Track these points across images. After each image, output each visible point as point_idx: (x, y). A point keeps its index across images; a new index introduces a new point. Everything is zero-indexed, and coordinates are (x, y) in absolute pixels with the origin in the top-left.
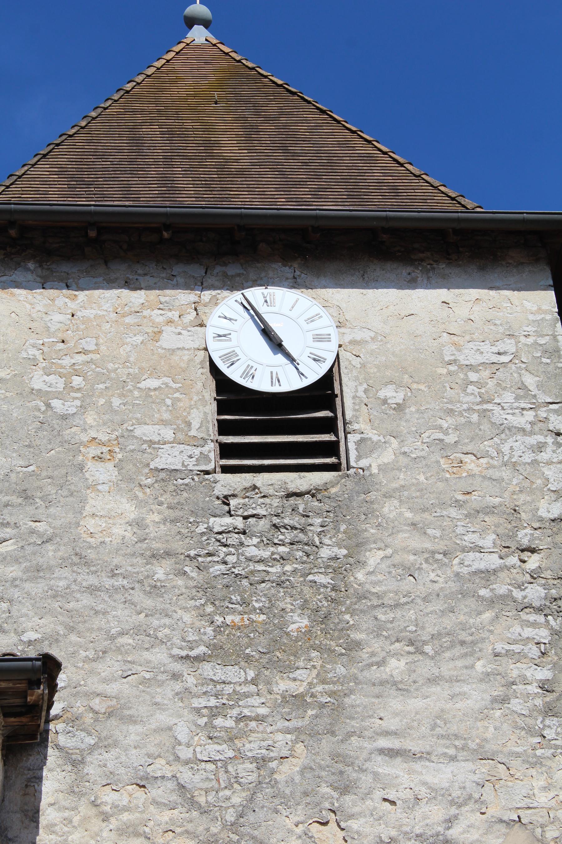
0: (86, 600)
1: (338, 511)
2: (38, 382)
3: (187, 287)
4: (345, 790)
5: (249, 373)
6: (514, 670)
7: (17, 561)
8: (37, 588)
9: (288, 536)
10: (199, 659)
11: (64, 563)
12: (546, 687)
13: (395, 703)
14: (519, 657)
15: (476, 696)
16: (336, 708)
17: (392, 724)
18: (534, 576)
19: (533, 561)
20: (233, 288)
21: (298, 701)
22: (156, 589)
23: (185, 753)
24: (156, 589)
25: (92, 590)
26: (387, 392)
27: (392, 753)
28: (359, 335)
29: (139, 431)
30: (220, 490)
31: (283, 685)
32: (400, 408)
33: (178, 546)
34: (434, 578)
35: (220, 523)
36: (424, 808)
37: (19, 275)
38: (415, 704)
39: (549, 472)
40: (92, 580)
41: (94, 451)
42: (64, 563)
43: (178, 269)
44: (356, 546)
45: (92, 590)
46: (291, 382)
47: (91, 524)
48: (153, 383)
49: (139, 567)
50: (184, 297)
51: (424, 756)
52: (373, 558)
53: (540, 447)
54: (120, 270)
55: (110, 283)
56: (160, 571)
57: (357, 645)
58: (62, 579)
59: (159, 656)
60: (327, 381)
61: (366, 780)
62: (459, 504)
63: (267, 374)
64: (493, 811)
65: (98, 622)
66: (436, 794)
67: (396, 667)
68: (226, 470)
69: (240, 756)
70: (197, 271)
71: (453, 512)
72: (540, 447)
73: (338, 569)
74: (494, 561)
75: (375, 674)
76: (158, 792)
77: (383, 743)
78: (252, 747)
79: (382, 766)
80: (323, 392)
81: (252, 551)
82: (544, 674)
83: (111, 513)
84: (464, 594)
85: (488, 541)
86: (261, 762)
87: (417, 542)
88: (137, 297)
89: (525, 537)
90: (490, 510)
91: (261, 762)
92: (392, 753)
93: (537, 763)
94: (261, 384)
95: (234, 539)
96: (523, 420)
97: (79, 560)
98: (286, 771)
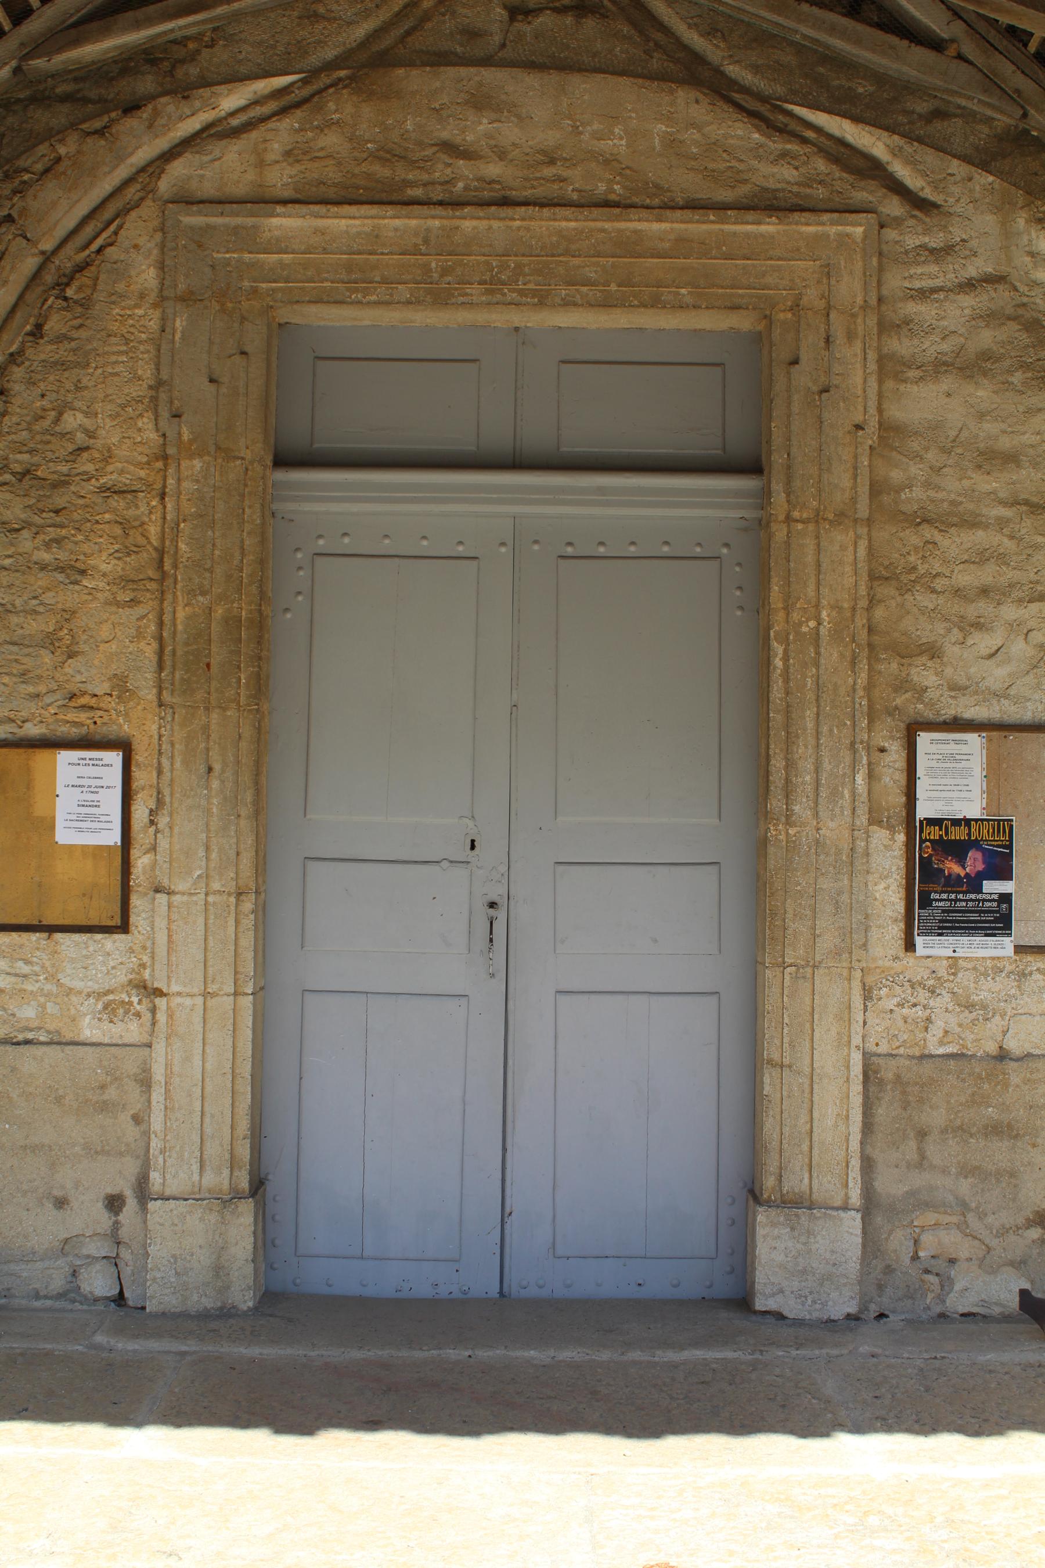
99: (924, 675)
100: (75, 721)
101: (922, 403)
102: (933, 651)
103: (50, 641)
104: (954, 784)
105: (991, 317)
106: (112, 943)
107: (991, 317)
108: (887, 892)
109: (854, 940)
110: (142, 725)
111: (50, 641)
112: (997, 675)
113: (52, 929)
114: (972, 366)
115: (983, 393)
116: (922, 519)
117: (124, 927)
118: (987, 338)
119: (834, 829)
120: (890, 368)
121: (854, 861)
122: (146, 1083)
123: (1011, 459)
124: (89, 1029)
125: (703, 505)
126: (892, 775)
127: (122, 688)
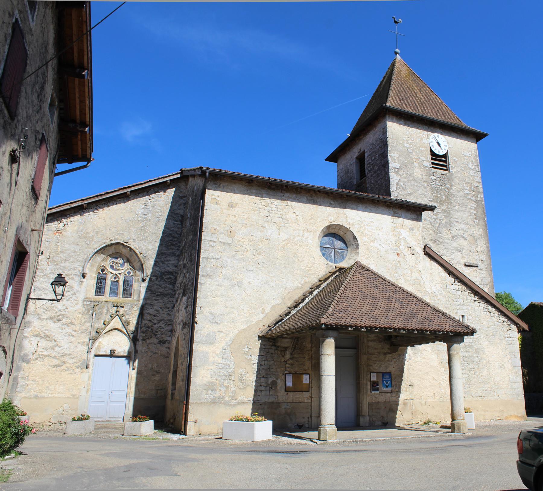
0: (415, 188)
1: (449, 179)
2: (406, 145)
3: (426, 130)
4: (451, 226)
5: (435, 150)
6: (471, 211)
7: (406, 178)
8: (409, 184)
9: (442, 182)
10: (431, 201)
11: (412, 180)
12: (475, 214)
13: (457, 214)
14: (472, 209)
15: (467, 214)
16: (449, 213)
17: (456, 217)
18: (474, 195)
19: (474, 193)
20: (432, 132)
21: (445, 211)
22: (425, 188)
23: (430, 217)
24: (425, 188)
25: (417, 186)
26: (454, 158)
27: (457, 222)
28: (451, 146)
29: (421, 158)
30: (432, 171)
31: (442, 208)
32: (456, 161)
33: (427, 180)
34: (461, 193)
35: (433, 177)
36: (461, 231)
37: (401, 122)
38: (459, 214)
39: (476, 178)
40: (416, 184)
41: (414, 160)
42: (412, 180)
43: (424, 126)
44: (451, 186)
45: (417, 186)
46: (441, 153)
47: (415, 174)
48: (422, 149)
49: (422, 183)
50: (426, 132)
51: (460, 223)
52: (454, 188)
53: (475, 173)
54: (416, 125)
55: (415, 127)
56: (425, 184)
57: (451, 203)
58: (412, 183)
59: (426, 199)
60: (446, 154)
61: (453, 225)
62: (464, 181)
63: (439, 151)
64: (469, 233)
65: (418, 192)
66: (462, 229)
67: (457, 207)
68: (433, 167)
69: (437, 218)
70: (427, 127)
71: (463, 182)
72: (475, 173)
73: (450, 189)
74: (468, 192)
75: (454, 208)
76: (428, 222)
77: (455, 220)
78: (439, 217)
79: (455, 223)
80: (445, 156)
81: (437, 183)
82: (475, 212)
83: (418, 173)
84: (466, 197)
85: (468, 188)
86: (440, 220)
87: (459, 187)
88: (419, 131)
89: (473, 188)
90: (468, 183)
91: (440, 220)
92: (457, 222)
93: (474, 226)
94: (437, 152)
95: (435, 181)
96: (473, 168)
97: (414, 180)
98: (443, 222)
99: (371, 368)
100: (305, 372)
101: (371, 344)
102: (372, 366)
103: (302, 364)
104: (374, 378)
105: (375, 336)
106: (308, 393)
107: (375, 336)
108: (369, 387)
109: (367, 392)
110: (310, 373)
111: (302, 364)
112: (377, 368)
113: (302, 391)
114: (374, 341)
115: (375, 343)
116: (370, 354)
117: (309, 391)
118: (375, 338)
119: (365, 382)
120: (368, 341)
121: (367, 384)
122: (311, 406)
123: (377, 349)
124: (306, 401)
125: (351, 352)
126: (369, 377)
127: (308, 369)
